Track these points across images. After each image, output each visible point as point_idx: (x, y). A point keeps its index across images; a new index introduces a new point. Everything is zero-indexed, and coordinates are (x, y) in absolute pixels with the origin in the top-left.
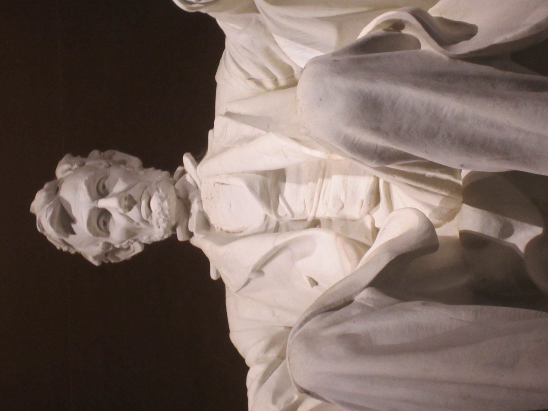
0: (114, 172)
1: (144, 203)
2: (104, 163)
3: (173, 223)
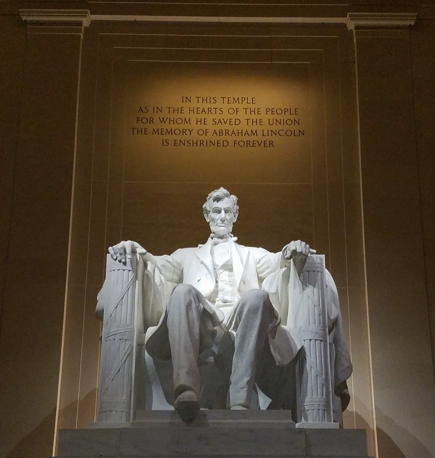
0: (232, 215)
1: (223, 225)
2: (235, 212)
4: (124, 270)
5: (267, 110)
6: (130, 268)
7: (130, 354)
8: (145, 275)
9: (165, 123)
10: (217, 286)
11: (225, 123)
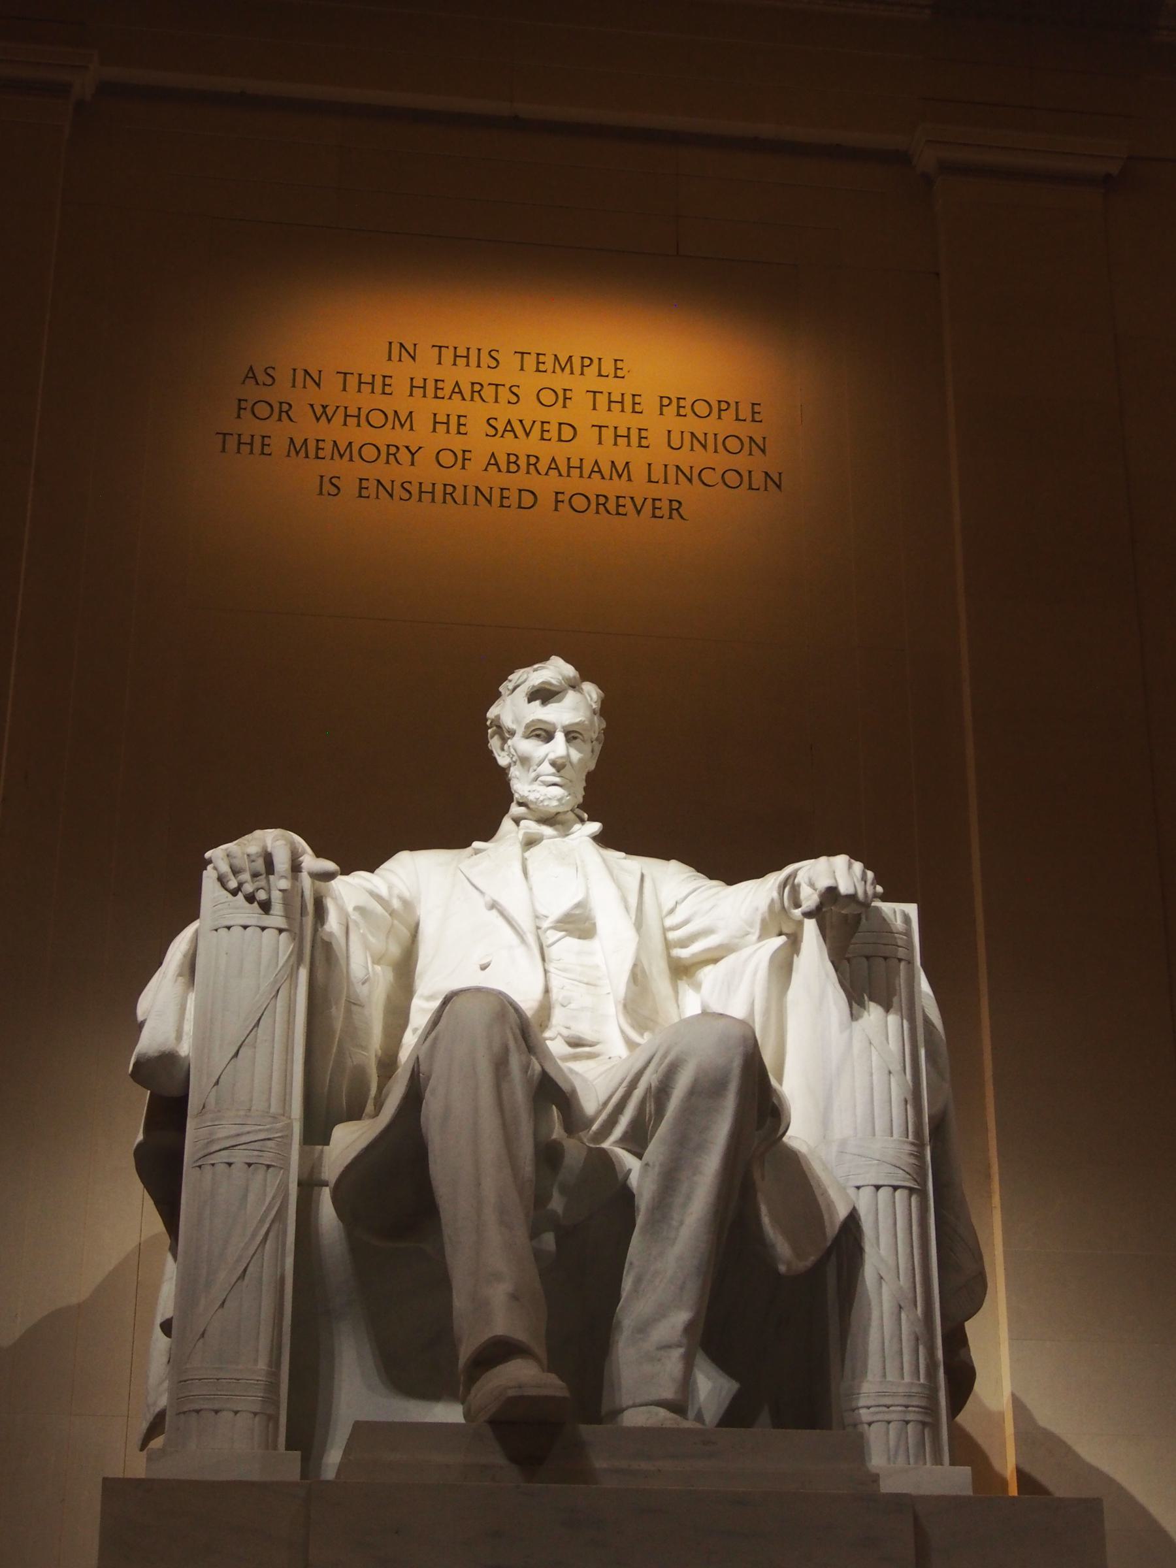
3: (531, 806)
4: (263, 929)
5: (664, 403)
6: (281, 922)
7: (281, 1215)
8: (319, 944)
9: (329, 421)
10: (547, 991)
11: (527, 435)
